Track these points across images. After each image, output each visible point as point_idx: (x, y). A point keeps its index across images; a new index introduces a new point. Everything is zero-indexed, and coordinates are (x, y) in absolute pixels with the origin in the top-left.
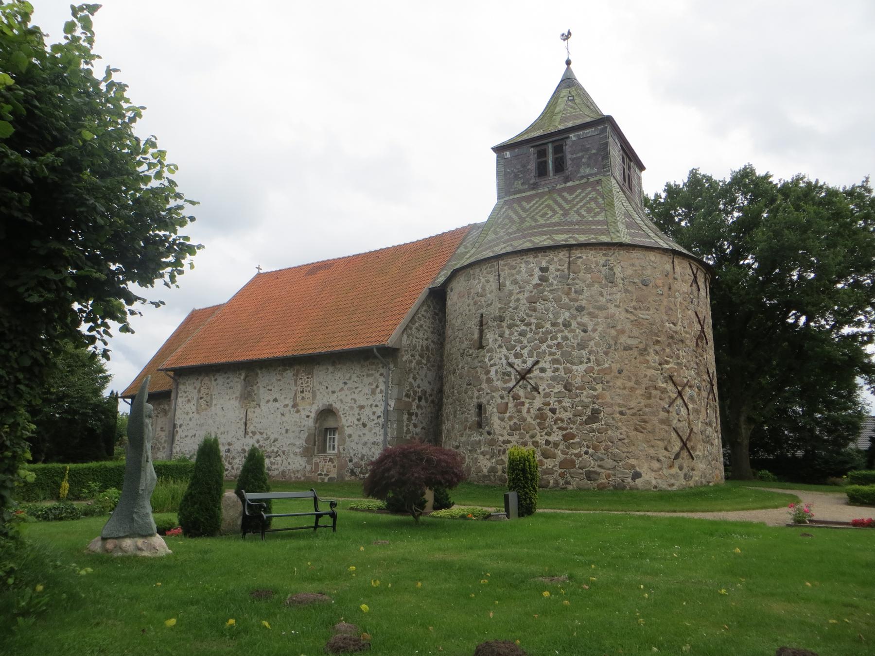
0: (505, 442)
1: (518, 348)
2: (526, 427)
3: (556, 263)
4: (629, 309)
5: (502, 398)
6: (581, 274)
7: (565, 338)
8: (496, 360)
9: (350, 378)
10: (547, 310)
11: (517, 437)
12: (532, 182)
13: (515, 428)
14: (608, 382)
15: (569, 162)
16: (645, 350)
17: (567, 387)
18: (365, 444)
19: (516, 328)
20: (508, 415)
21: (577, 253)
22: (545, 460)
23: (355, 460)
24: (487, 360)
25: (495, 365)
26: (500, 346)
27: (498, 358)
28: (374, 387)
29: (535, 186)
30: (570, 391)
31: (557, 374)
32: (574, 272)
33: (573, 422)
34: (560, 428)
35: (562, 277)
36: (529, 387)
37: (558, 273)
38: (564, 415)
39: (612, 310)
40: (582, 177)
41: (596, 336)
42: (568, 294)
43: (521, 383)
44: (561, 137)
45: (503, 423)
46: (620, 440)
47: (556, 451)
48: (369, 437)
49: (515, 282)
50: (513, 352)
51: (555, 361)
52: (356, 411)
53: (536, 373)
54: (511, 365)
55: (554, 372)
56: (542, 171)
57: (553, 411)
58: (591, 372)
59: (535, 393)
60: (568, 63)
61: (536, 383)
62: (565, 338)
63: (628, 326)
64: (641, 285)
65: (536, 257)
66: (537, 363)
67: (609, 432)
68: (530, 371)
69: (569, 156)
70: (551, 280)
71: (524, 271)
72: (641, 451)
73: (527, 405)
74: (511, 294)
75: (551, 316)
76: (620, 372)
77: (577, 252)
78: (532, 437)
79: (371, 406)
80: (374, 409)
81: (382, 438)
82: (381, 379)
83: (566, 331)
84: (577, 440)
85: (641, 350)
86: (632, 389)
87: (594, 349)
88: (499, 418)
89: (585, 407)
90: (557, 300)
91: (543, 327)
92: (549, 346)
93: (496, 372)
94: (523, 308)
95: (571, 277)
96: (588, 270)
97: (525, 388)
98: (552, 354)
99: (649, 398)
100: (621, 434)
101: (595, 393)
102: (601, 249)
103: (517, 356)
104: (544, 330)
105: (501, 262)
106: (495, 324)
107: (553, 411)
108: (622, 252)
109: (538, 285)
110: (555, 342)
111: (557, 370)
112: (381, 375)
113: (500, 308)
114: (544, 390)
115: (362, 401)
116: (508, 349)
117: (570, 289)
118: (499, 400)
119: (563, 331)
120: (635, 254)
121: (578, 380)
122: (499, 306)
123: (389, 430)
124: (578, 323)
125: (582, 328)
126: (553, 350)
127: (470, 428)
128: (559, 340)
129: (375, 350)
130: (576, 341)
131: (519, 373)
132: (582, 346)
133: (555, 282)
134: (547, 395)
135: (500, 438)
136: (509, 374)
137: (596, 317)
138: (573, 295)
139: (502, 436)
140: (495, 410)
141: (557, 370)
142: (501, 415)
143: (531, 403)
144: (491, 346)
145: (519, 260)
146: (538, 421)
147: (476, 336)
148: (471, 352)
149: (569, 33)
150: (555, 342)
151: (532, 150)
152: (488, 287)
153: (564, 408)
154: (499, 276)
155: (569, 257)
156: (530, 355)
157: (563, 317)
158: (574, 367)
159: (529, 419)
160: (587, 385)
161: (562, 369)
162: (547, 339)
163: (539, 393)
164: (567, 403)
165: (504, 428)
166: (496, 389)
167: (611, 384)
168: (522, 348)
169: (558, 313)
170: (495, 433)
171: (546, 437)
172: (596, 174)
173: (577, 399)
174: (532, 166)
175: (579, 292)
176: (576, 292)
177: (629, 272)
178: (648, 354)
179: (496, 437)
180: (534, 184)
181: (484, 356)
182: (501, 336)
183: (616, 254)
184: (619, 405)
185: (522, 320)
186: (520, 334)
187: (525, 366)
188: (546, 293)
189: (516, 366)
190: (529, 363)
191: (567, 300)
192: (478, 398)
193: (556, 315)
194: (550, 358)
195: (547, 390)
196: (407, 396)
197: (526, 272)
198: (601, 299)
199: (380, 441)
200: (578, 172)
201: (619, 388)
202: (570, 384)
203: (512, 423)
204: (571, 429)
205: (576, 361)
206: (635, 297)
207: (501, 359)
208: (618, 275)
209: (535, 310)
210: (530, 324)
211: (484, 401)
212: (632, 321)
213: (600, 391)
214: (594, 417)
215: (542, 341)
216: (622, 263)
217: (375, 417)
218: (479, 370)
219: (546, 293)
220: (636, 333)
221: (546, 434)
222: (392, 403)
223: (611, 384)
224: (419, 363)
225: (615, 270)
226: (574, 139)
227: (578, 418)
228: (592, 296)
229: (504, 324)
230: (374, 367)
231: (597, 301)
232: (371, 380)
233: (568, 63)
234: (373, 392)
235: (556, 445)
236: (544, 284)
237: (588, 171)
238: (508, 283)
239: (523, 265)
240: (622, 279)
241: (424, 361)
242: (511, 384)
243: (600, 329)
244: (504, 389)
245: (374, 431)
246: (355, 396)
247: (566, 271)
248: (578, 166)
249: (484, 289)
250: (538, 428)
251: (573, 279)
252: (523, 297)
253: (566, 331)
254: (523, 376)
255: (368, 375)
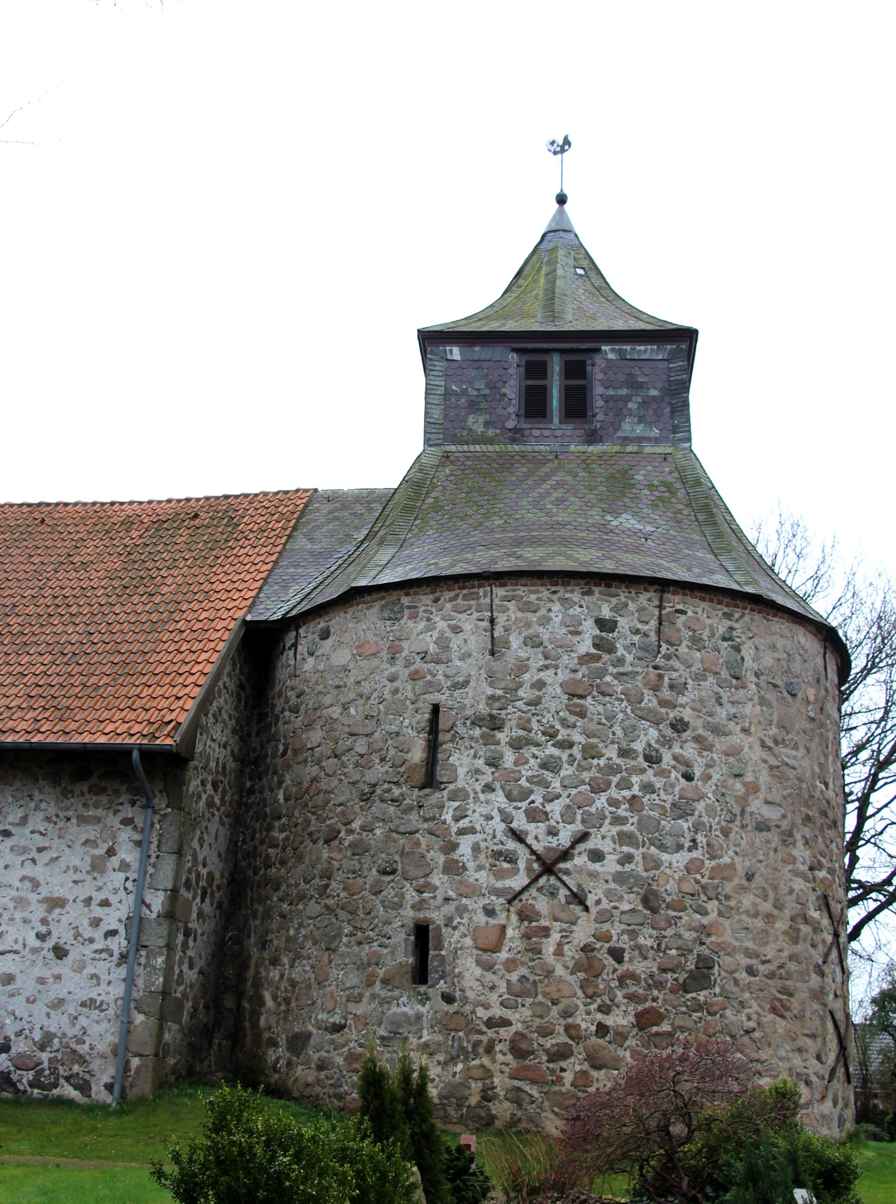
0: (491, 1023)
1: (537, 798)
2: (552, 989)
3: (634, 615)
4: (767, 740)
5: (490, 912)
6: (683, 649)
7: (648, 788)
8: (475, 818)
9: (24, 821)
10: (611, 717)
11: (527, 1012)
12: (510, 424)
13: (521, 992)
14: (728, 898)
15: (599, 403)
16: (790, 834)
17: (650, 901)
18: (59, 1004)
19: (534, 750)
20: (504, 955)
21: (674, 601)
22: (594, 1074)
23: (20, 1047)
24: (448, 816)
25: (472, 830)
26: (489, 788)
27: (480, 811)
28: (100, 851)
29: (516, 435)
30: (654, 911)
31: (628, 868)
32: (669, 643)
33: (660, 985)
34: (632, 998)
35: (644, 648)
36: (563, 892)
37: (636, 638)
38: (640, 967)
39: (738, 738)
40: (626, 440)
41: (708, 789)
42: (656, 689)
43: (542, 881)
44: (585, 346)
45: (489, 977)
46: (747, 1032)
47: (621, 1053)
48: (73, 985)
49: (533, 642)
50: (524, 805)
51: (624, 838)
52: (40, 912)
53: (580, 860)
54: (518, 836)
55: (621, 862)
56: (535, 406)
57: (617, 955)
58: (698, 871)
59: (577, 909)
60: (562, 200)
61: (579, 886)
62: (648, 788)
63: (764, 778)
64: (785, 694)
65: (589, 593)
66: (583, 837)
67: (728, 1012)
68: (565, 855)
69: (598, 390)
70: (621, 651)
71: (558, 620)
72: (781, 1059)
73: (555, 937)
74: (522, 667)
75: (619, 732)
76: (749, 877)
77: (677, 598)
78: (567, 1014)
79: (88, 901)
80: (98, 912)
81: (119, 990)
82: (126, 835)
83: (650, 772)
84: (665, 1027)
85: (783, 833)
86: (769, 918)
87: (705, 819)
88: (479, 963)
89: (684, 951)
90: (634, 699)
91: (599, 756)
92: (613, 802)
93: (476, 849)
94: (553, 706)
95: (663, 650)
96: (696, 642)
97: (553, 895)
98: (618, 820)
99: (795, 941)
100: (749, 1018)
101: (705, 921)
102: (720, 602)
103: (533, 815)
104: (602, 762)
105: (500, 592)
106: (477, 732)
107: (617, 955)
108: (757, 616)
109: (587, 659)
110: (626, 793)
111: (629, 858)
112: (127, 822)
113: (492, 698)
114: (598, 902)
115: (57, 883)
116: (509, 797)
117: (661, 677)
118: (481, 918)
119: (643, 771)
120: (779, 625)
121: (671, 886)
122: (489, 691)
123: (140, 970)
124: (675, 758)
125: (683, 769)
126: (622, 812)
127: (385, 982)
128: (636, 790)
129: (136, 754)
130: (670, 799)
131: (539, 858)
132: (681, 809)
133: (629, 658)
134: (605, 917)
135: (481, 1012)
136: (511, 858)
137: (710, 748)
138: (666, 694)
139: (487, 1007)
140: (468, 941)
141: (629, 858)
142: (485, 957)
143: (566, 935)
144: (460, 783)
145: (545, 594)
146: (581, 975)
147: (417, 754)
148: (396, 792)
149: (567, 142)
150: (626, 793)
151: (513, 357)
152: (456, 642)
153: (639, 947)
154: (492, 621)
155: (660, 607)
156: (568, 816)
157: (644, 739)
158: (665, 857)
159: (559, 971)
160: (688, 901)
161: (638, 858)
162: (608, 784)
163: (587, 909)
164: (646, 940)
165: (493, 988)
166: (473, 891)
167: (732, 903)
168: (550, 798)
169: (634, 728)
170: (465, 1000)
171: (599, 1016)
172: (656, 441)
173: (669, 932)
174: (512, 390)
175: (678, 688)
176: (672, 687)
177: (768, 660)
178: (794, 844)
179: (468, 1008)
180: (516, 430)
181: (442, 807)
182: (494, 762)
183: (747, 618)
184: (749, 954)
185: (551, 734)
186: (544, 766)
187: (554, 842)
188: (608, 678)
189: (530, 840)
190: (565, 838)
191: (654, 703)
192: (418, 906)
193: (630, 732)
194: (615, 830)
195: (605, 905)
196: (188, 885)
197: (563, 623)
198: (718, 709)
199: (110, 998)
200: (618, 428)
201: (747, 912)
202: (655, 894)
203: (514, 977)
204: (655, 999)
205: (669, 841)
206: (775, 718)
207: (489, 818)
208: (749, 663)
209: (582, 714)
210: (571, 745)
211: (436, 916)
212: (771, 768)
213: (713, 915)
214: (701, 975)
215: (598, 788)
216: (757, 640)
217: (98, 934)
218: (424, 840)
219: (608, 678)
220: (776, 796)
221: (600, 1009)
222: (157, 901)
223: (732, 903)
224: (210, 804)
225: (744, 652)
226: (611, 356)
227: (669, 976)
228: (701, 700)
229: (502, 736)
230: (104, 799)
231: (711, 715)
232: (91, 831)
233: (562, 200)
234: (97, 867)
235: (621, 1037)
236: (606, 657)
237: (639, 430)
238: (515, 641)
239: (556, 607)
240: (757, 675)
241: (217, 801)
242: (518, 882)
243: (716, 777)
244: (498, 892)
245: (90, 970)
246: (38, 871)
247: (653, 637)
248: (620, 416)
249: (443, 643)
250: (580, 993)
251: (668, 657)
252: (556, 680)
253: (650, 772)
254: (549, 865)
255: (82, 820)
